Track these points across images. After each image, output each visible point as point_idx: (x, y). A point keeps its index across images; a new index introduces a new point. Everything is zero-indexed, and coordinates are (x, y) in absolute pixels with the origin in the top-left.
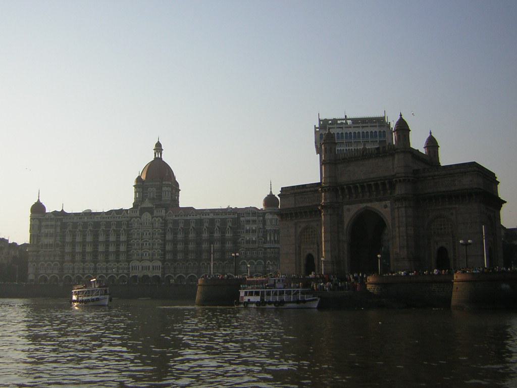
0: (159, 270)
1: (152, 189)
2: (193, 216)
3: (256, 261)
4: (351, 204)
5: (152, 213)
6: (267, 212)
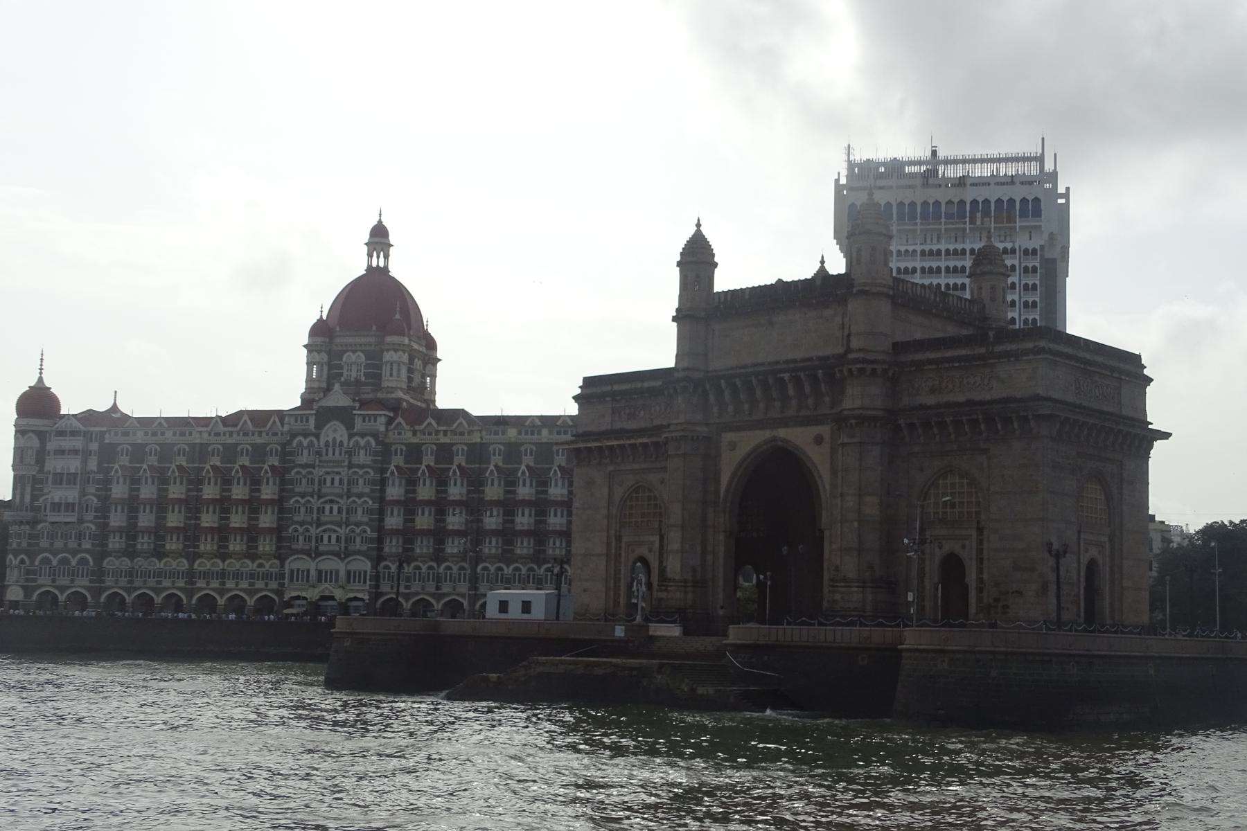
0: (365, 582)
1: (354, 357)
2: (462, 434)
5: (349, 425)
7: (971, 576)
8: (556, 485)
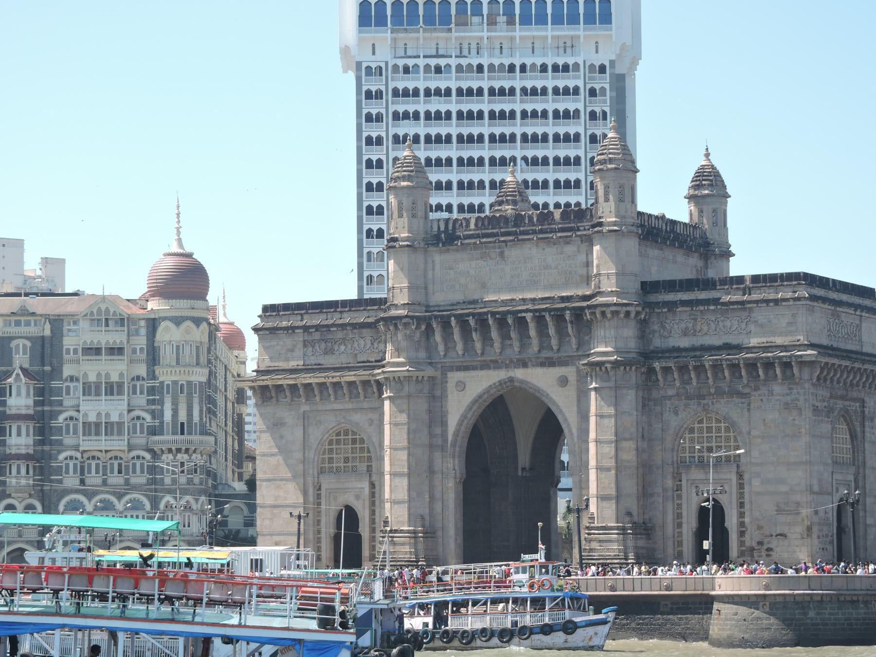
3: (120, 497)
4: (466, 368)
6: (165, 319)
7: (731, 522)
8: (19, 394)
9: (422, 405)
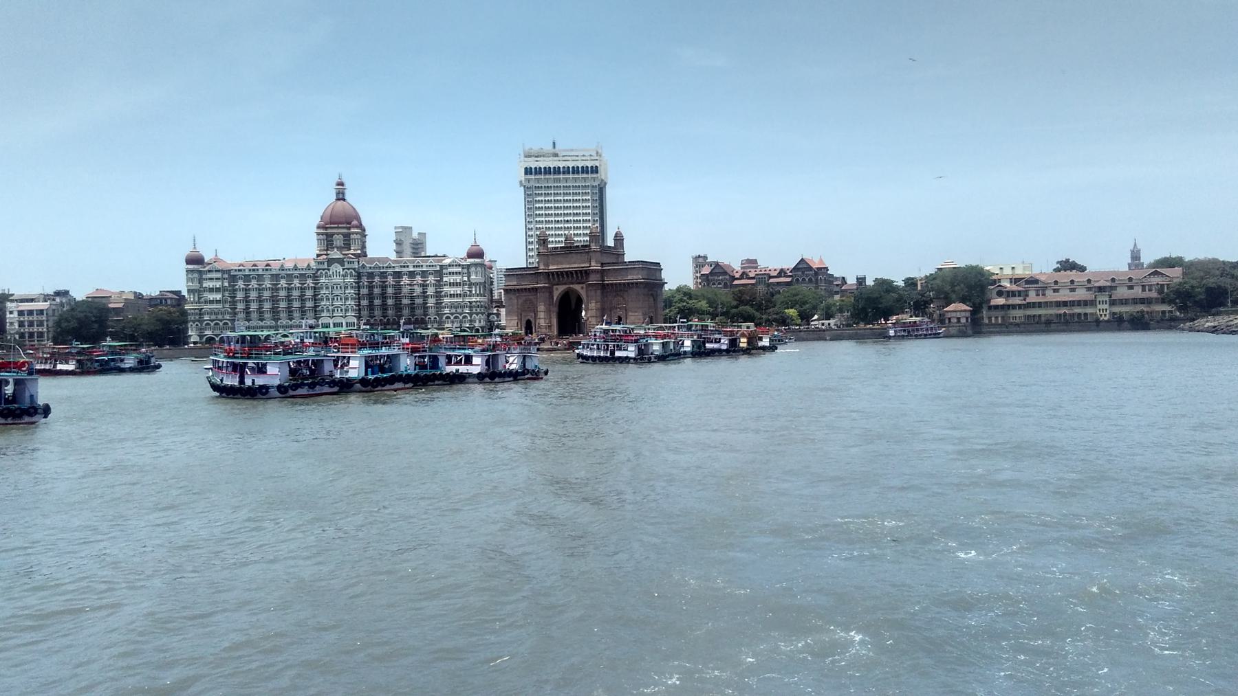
1: (338, 237)
2: (390, 267)
9: (547, 294)
